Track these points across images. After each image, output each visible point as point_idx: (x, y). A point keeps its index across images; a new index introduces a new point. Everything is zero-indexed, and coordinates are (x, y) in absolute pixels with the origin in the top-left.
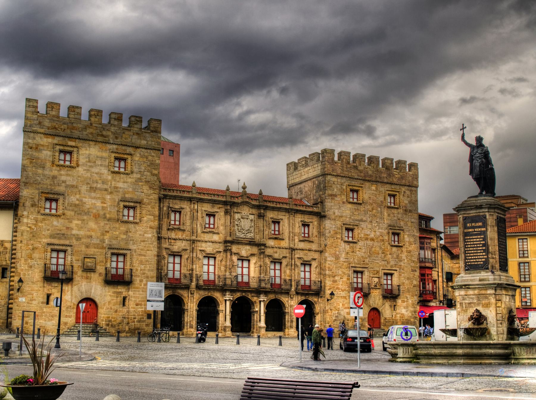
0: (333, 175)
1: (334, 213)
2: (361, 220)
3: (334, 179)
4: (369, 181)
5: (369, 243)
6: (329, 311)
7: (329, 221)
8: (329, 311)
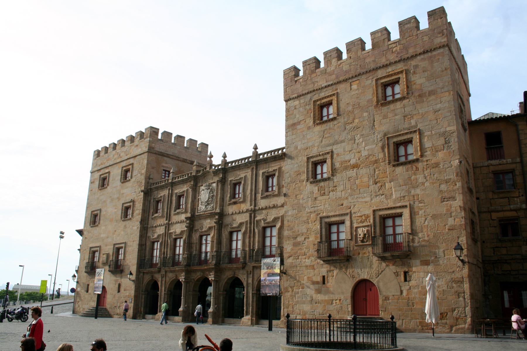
0: (293, 98)
1: (296, 148)
2: (336, 143)
3: (297, 102)
4: (345, 80)
5: (352, 173)
6: (290, 289)
7: (289, 160)
8: (290, 289)
